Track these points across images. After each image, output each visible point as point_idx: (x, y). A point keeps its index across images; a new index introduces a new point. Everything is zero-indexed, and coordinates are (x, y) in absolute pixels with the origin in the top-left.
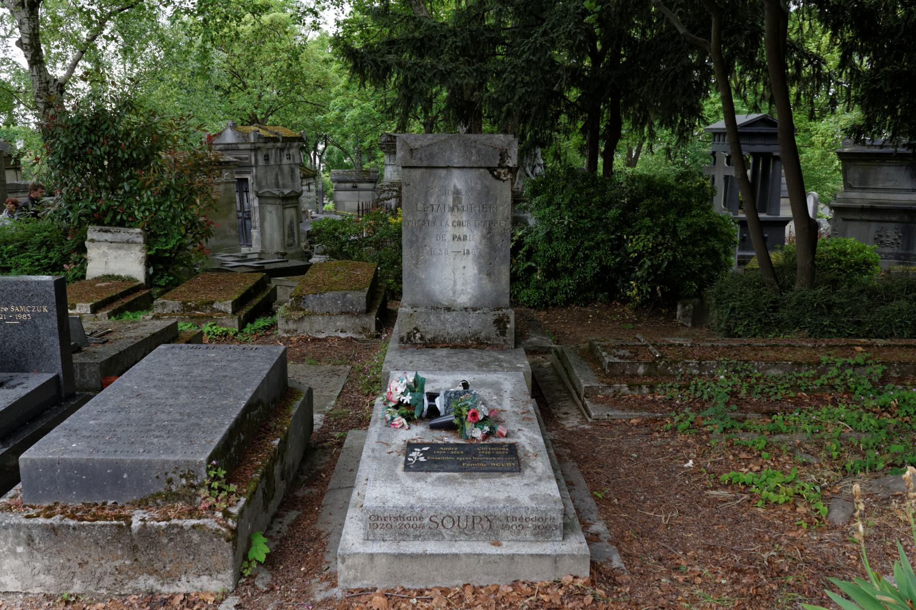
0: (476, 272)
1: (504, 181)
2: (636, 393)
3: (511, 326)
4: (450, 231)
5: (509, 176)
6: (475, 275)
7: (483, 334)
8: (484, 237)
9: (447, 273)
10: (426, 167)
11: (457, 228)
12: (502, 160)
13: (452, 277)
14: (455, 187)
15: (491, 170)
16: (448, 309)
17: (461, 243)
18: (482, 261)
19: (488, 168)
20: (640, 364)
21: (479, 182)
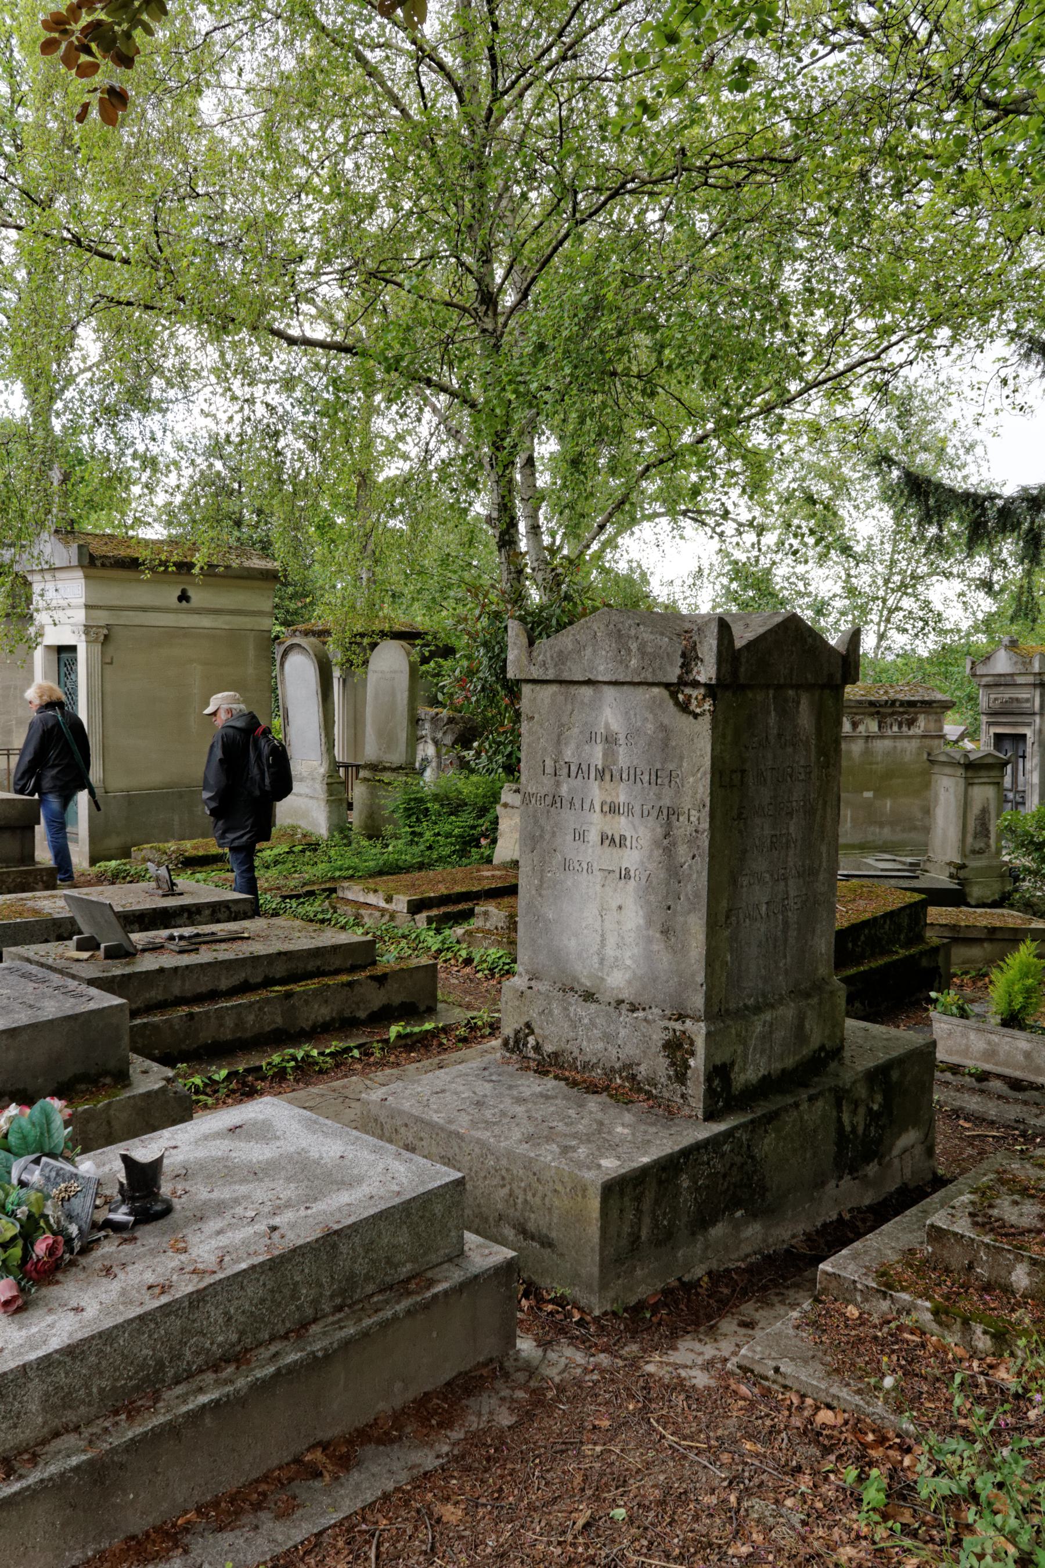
0: (642, 922)
1: (696, 716)
2: (951, 1340)
3: (697, 1063)
4: (596, 823)
5: (706, 707)
6: (638, 927)
7: (642, 1068)
8: (656, 843)
9: (590, 913)
10: (561, 682)
11: (609, 816)
12: (686, 666)
13: (597, 925)
14: (607, 726)
15: (673, 689)
16: (589, 996)
17: (616, 851)
18: (652, 898)
19: (667, 686)
20: (1019, 1258)
21: (651, 717)
